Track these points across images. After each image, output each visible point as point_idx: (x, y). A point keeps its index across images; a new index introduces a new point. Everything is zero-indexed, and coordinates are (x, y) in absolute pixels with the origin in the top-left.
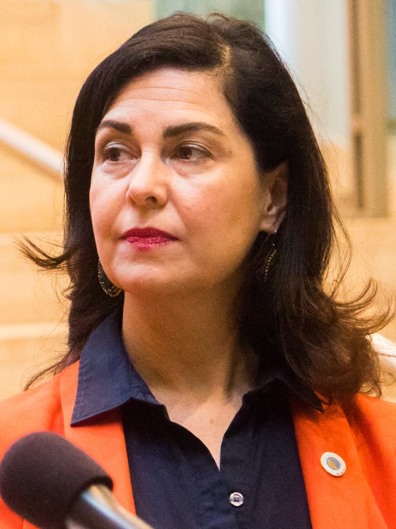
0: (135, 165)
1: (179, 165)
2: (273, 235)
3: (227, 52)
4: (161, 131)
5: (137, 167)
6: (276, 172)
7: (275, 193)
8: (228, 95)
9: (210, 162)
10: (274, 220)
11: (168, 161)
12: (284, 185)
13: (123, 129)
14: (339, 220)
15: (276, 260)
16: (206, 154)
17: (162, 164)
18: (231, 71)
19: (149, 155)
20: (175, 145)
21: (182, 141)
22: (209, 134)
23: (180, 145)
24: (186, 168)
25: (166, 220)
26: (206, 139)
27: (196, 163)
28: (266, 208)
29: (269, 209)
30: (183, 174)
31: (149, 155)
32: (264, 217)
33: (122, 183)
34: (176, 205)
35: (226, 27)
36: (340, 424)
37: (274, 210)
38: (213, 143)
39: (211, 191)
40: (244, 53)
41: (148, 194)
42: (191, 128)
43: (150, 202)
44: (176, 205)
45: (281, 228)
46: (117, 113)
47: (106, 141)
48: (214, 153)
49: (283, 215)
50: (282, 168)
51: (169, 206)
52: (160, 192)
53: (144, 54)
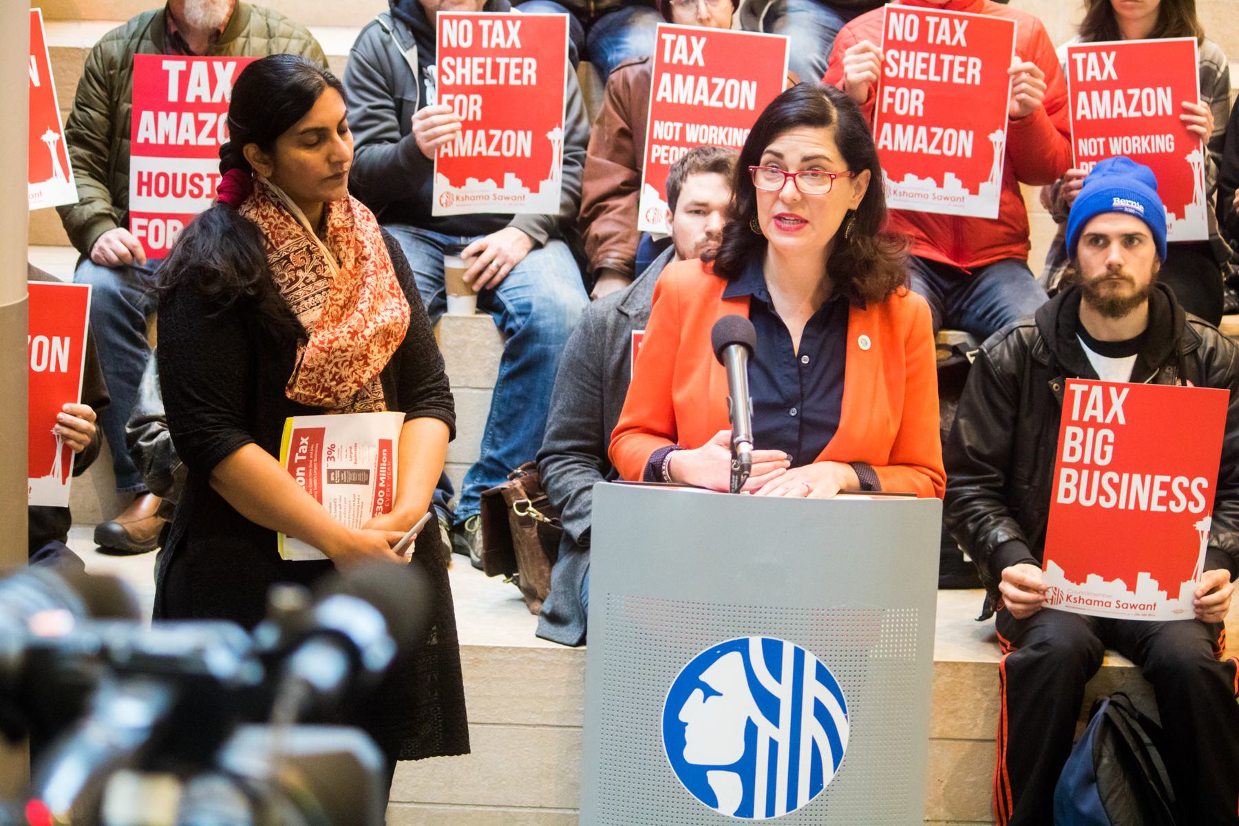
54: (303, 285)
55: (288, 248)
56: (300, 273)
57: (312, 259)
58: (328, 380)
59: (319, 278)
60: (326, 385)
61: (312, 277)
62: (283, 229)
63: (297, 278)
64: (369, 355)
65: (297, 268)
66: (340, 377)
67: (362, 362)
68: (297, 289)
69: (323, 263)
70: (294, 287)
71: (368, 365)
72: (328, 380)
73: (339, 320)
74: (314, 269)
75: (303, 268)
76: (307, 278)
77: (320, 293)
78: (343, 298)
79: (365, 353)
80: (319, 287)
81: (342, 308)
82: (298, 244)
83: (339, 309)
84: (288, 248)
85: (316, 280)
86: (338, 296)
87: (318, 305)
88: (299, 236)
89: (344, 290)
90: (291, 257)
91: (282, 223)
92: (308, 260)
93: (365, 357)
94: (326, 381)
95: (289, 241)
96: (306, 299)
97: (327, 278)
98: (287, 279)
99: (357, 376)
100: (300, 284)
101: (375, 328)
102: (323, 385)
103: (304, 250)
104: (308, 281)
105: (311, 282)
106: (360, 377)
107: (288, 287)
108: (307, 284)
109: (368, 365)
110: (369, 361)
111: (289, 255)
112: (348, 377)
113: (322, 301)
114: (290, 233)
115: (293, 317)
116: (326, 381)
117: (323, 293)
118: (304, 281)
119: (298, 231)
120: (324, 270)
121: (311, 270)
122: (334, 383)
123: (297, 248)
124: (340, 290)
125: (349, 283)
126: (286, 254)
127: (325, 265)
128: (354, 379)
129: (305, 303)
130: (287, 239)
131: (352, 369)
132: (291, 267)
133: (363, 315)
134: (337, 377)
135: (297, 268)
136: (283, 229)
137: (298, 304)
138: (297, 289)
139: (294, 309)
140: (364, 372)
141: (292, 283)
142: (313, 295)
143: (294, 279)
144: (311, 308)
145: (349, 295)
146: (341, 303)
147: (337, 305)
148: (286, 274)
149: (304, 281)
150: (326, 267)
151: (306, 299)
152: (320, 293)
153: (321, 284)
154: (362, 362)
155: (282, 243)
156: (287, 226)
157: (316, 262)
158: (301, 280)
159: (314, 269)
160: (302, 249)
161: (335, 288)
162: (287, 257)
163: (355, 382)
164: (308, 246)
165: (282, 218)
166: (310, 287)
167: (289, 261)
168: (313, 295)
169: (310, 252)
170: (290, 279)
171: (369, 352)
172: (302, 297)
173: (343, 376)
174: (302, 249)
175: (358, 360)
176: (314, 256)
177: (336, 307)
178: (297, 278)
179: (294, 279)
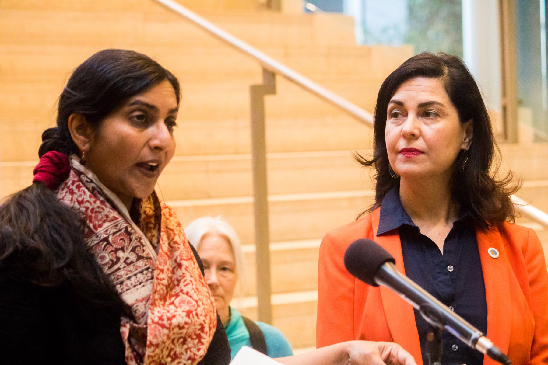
0: (405, 120)
1: (425, 120)
2: (467, 151)
3: (446, 70)
4: (417, 105)
5: (406, 121)
6: (468, 123)
7: (467, 132)
8: (447, 89)
9: (439, 119)
10: (467, 144)
11: (420, 118)
12: (471, 129)
13: (400, 104)
14: (496, 144)
15: (468, 162)
16: (437, 115)
17: (417, 119)
18: (448, 78)
19: (412, 116)
20: (423, 111)
21: (426, 109)
22: (438, 106)
23: (425, 111)
24: (428, 121)
25: (419, 144)
26: (437, 108)
27: (432, 119)
28: (464, 139)
29: (465, 139)
30: (426, 124)
31: (412, 116)
32: (463, 143)
33: (399, 128)
34: (423, 137)
35: (446, 58)
36: (497, 235)
37: (467, 140)
38: (440, 110)
39: (439, 131)
40: (454, 70)
41: (411, 133)
42: (430, 104)
43: (412, 136)
44: (423, 137)
45: (470, 148)
46: (397, 97)
47: (392, 109)
48: (440, 114)
49: (471, 142)
50: (471, 121)
51: (421, 138)
52: (416, 132)
53: (409, 71)
54: (124, 265)
55: (107, 231)
56: (120, 254)
57: (131, 240)
58: (165, 357)
59: (139, 258)
60: (163, 361)
61: (133, 257)
62: (100, 212)
63: (118, 259)
64: (202, 335)
65: (116, 250)
66: (175, 353)
67: (196, 341)
68: (119, 269)
69: (142, 244)
70: (116, 267)
71: (203, 344)
72: (165, 357)
73: (165, 300)
74: (133, 250)
75: (122, 249)
76: (127, 258)
77: (142, 272)
78: (166, 278)
79: (198, 332)
80: (140, 267)
81: (167, 287)
82: (116, 226)
83: (165, 288)
84: (107, 231)
85: (137, 260)
86: (162, 276)
87: (140, 283)
88: (116, 218)
89: (165, 270)
90: (110, 239)
91: (98, 207)
92: (127, 241)
93: (199, 337)
94: (163, 357)
95: (107, 224)
96: (129, 278)
97: (147, 258)
98: (107, 260)
99: (192, 354)
100: (121, 264)
101: (204, 309)
102: (160, 361)
103: (123, 231)
104: (129, 261)
105: (132, 262)
106: (195, 354)
107: (110, 268)
108: (128, 264)
109: (203, 344)
110: (203, 340)
111: (108, 237)
112: (182, 354)
113: (144, 281)
114: (107, 216)
115: (117, 296)
116: (163, 357)
117: (145, 272)
118: (125, 262)
119: (115, 214)
120: (144, 251)
121: (131, 251)
122: (169, 359)
123: (115, 230)
124: (162, 271)
125: (168, 264)
126: (105, 236)
127: (143, 246)
128: (188, 355)
129: (128, 282)
130: (104, 222)
131: (185, 347)
132: (111, 248)
133: (191, 297)
134: (172, 353)
135: (116, 250)
136: (100, 212)
137: (122, 283)
138: (119, 269)
139: (118, 287)
140: (199, 350)
141: (114, 263)
142: (135, 275)
143: (115, 260)
144: (135, 286)
145: (170, 275)
146: (165, 282)
147: (163, 284)
148: (107, 255)
149: (125, 262)
150: (144, 248)
151: (129, 278)
152: (142, 272)
153: (141, 263)
154: (196, 341)
155: (100, 226)
156: (103, 209)
157: (134, 243)
158: (122, 261)
159: (133, 250)
160: (120, 230)
161: (157, 268)
162: (106, 239)
163: (189, 358)
164: (126, 228)
165: (98, 203)
166: (131, 268)
167: (108, 243)
168: (135, 275)
169: (129, 234)
170: (112, 260)
171: (203, 332)
172: (125, 277)
173: (178, 352)
174: (120, 230)
175: (192, 339)
176: (133, 237)
177: (161, 286)
178: (118, 259)
179: (115, 260)
